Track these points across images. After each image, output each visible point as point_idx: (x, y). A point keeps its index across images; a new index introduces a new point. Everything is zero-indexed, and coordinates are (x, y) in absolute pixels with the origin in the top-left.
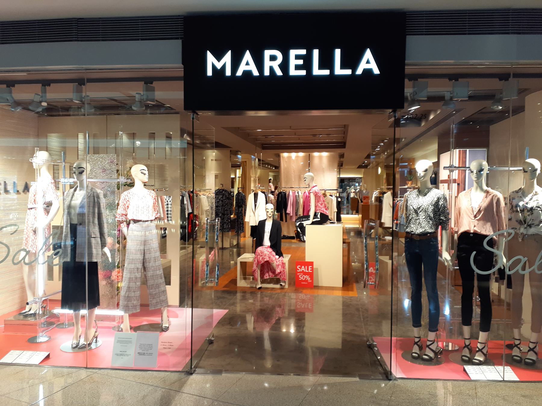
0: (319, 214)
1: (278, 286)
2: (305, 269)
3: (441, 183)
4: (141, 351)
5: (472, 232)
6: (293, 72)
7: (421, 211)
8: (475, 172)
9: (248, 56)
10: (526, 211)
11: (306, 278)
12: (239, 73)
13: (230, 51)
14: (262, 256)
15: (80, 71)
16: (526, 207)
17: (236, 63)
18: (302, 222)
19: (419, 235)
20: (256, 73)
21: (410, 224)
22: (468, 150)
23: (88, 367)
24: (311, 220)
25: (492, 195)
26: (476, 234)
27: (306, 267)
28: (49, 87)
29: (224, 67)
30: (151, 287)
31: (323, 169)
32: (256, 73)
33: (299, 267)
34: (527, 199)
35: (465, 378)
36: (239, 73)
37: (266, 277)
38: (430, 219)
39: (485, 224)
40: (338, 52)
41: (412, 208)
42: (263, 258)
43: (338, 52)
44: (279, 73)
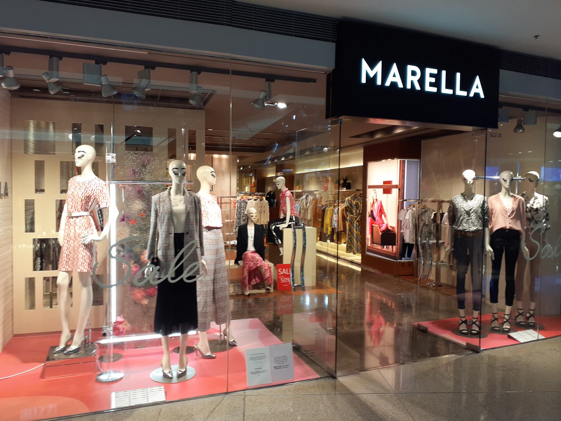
0: (294, 217)
1: (263, 291)
2: (286, 271)
3: (369, 188)
4: (276, 365)
5: (508, 228)
6: (428, 88)
7: (472, 213)
8: (508, 181)
9: (394, 69)
10: (532, 211)
11: (287, 281)
12: (388, 84)
13: (381, 61)
14: (253, 261)
15: (249, 62)
16: (533, 208)
17: (385, 73)
18: (278, 226)
19: (473, 232)
20: (401, 85)
21: (462, 223)
22: (406, 160)
23: (229, 391)
24: (287, 222)
25: (519, 199)
26: (511, 230)
27: (287, 269)
28: (7, 56)
29: (375, 76)
30: (220, 299)
31: (223, 171)
32: (401, 85)
33: (280, 270)
34: (531, 202)
35: (515, 343)
36: (388, 84)
37: (254, 282)
38: (480, 219)
39: (516, 222)
40: (458, 75)
41: (463, 210)
42: (254, 263)
43: (458, 75)
44: (418, 87)
